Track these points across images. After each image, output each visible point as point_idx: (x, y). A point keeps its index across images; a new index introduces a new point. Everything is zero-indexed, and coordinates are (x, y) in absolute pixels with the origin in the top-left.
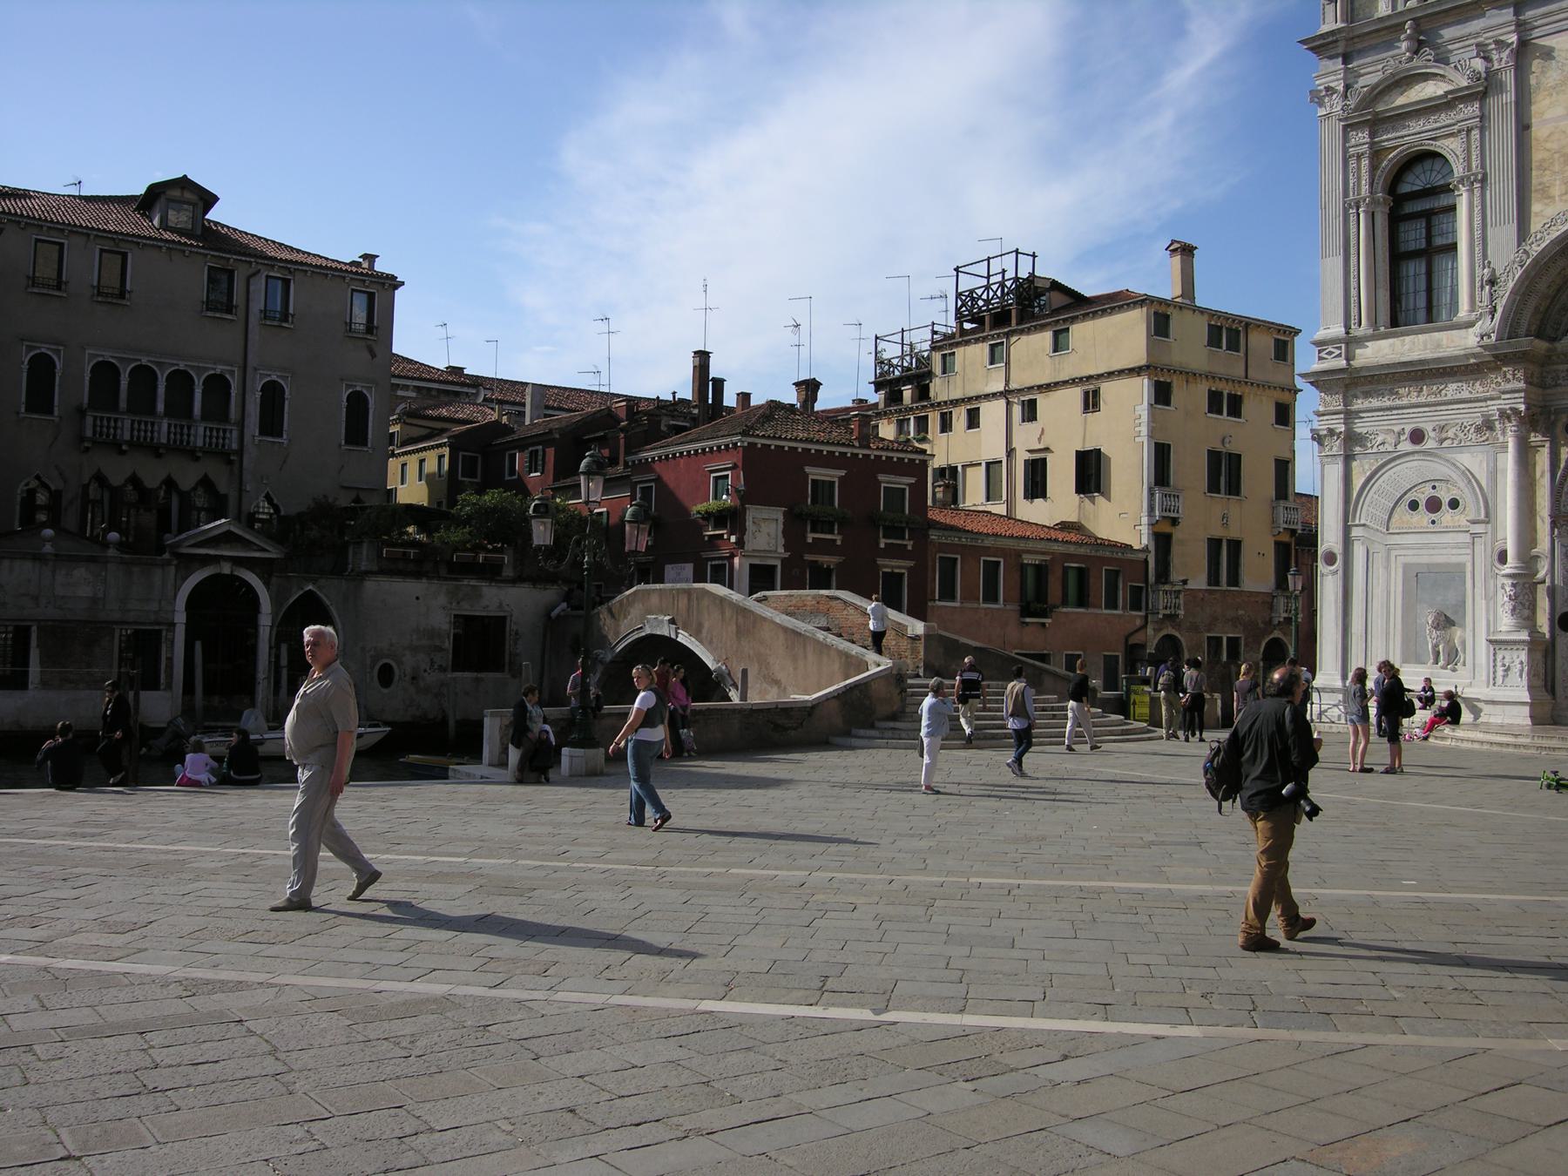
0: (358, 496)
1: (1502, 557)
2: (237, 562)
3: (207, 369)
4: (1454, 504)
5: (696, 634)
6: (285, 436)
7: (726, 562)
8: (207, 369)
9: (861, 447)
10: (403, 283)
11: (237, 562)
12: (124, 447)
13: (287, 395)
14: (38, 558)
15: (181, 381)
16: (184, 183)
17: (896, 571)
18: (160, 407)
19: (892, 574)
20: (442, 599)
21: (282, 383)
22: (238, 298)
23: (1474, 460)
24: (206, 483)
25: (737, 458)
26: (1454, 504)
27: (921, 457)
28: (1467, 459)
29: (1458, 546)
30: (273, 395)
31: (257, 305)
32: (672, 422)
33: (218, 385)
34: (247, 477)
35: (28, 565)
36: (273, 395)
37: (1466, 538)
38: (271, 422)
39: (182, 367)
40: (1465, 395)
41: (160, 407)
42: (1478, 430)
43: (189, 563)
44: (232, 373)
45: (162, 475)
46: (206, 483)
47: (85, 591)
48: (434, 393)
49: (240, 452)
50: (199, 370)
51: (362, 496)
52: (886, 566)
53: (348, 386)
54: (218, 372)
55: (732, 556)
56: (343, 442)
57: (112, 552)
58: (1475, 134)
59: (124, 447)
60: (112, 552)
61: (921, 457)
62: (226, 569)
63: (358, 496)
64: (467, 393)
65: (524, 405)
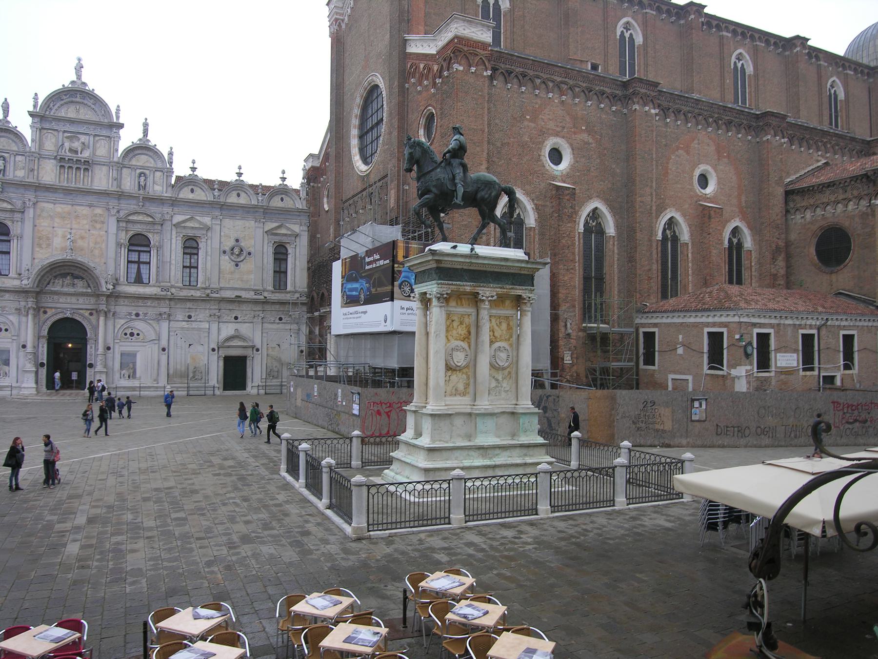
1: (24, 346)
4: (6, 330)
23: (14, 318)
26: (6, 330)
28: (11, 317)
29: (10, 342)
37: (10, 340)
40: (12, 299)
42: (16, 309)
58: (20, 223)
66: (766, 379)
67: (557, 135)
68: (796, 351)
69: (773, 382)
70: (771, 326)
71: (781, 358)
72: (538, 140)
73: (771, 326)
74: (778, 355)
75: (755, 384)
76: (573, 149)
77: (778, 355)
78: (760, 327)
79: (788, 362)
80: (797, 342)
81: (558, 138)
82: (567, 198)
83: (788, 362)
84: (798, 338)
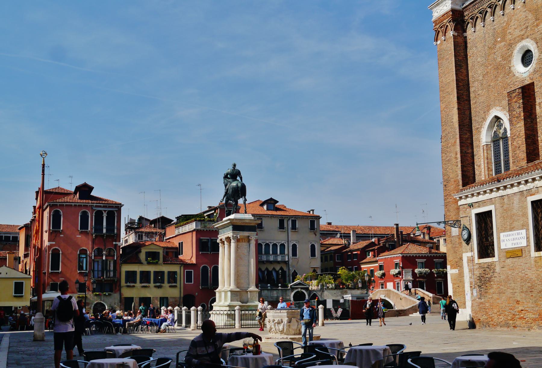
0: (314, 269)
2: (302, 288)
3: (280, 243)
5: (389, 298)
6: (297, 256)
7: (400, 282)
8: (280, 243)
9: (429, 254)
10: (321, 217)
11: (302, 288)
12: (265, 262)
13: (297, 246)
14: (268, 290)
15: (275, 246)
16: (271, 199)
17: (440, 281)
18: (271, 252)
19: (439, 282)
20: (340, 293)
21: (296, 244)
22: (285, 225)
24: (281, 269)
25: (400, 259)
27: (445, 255)
30: (294, 247)
31: (290, 226)
32: (390, 243)
33: (282, 246)
34: (290, 266)
35: (266, 291)
36: (294, 247)
38: (294, 254)
39: (275, 243)
41: (271, 252)
43: (292, 289)
44: (285, 243)
45: (272, 268)
46: (281, 269)
47: (276, 295)
48: (325, 234)
49: (288, 261)
50: (279, 243)
51: (315, 269)
52: (438, 281)
53: (311, 243)
54: (283, 243)
55: (400, 281)
56: (310, 256)
57: (280, 288)
59: (265, 262)
60: (280, 288)
61: (445, 255)
62: (299, 290)
63: (314, 269)
64: (334, 233)
65: (350, 234)
66: (490, 266)
67: (523, 39)
68: (524, 226)
69: (498, 269)
70: (490, 201)
71: (505, 238)
72: (508, 55)
73: (490, 201)
74: (502, 235)
75: (477, 273)
76: (537, 43)
77: (502, 235)
78: (479, 207)
79: (515, 242)
80: (525, 215)
81: (518, 45)
82: (514, 100)
83: (515, 242)
84: (526, 208)
